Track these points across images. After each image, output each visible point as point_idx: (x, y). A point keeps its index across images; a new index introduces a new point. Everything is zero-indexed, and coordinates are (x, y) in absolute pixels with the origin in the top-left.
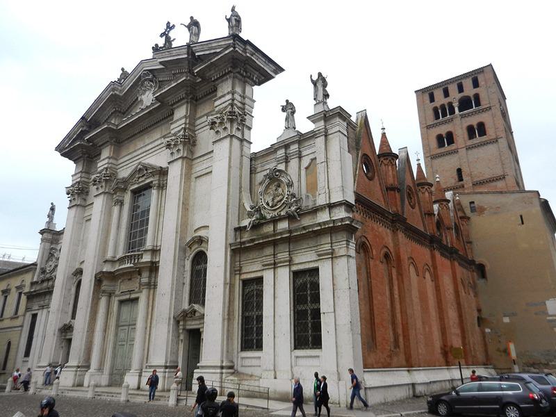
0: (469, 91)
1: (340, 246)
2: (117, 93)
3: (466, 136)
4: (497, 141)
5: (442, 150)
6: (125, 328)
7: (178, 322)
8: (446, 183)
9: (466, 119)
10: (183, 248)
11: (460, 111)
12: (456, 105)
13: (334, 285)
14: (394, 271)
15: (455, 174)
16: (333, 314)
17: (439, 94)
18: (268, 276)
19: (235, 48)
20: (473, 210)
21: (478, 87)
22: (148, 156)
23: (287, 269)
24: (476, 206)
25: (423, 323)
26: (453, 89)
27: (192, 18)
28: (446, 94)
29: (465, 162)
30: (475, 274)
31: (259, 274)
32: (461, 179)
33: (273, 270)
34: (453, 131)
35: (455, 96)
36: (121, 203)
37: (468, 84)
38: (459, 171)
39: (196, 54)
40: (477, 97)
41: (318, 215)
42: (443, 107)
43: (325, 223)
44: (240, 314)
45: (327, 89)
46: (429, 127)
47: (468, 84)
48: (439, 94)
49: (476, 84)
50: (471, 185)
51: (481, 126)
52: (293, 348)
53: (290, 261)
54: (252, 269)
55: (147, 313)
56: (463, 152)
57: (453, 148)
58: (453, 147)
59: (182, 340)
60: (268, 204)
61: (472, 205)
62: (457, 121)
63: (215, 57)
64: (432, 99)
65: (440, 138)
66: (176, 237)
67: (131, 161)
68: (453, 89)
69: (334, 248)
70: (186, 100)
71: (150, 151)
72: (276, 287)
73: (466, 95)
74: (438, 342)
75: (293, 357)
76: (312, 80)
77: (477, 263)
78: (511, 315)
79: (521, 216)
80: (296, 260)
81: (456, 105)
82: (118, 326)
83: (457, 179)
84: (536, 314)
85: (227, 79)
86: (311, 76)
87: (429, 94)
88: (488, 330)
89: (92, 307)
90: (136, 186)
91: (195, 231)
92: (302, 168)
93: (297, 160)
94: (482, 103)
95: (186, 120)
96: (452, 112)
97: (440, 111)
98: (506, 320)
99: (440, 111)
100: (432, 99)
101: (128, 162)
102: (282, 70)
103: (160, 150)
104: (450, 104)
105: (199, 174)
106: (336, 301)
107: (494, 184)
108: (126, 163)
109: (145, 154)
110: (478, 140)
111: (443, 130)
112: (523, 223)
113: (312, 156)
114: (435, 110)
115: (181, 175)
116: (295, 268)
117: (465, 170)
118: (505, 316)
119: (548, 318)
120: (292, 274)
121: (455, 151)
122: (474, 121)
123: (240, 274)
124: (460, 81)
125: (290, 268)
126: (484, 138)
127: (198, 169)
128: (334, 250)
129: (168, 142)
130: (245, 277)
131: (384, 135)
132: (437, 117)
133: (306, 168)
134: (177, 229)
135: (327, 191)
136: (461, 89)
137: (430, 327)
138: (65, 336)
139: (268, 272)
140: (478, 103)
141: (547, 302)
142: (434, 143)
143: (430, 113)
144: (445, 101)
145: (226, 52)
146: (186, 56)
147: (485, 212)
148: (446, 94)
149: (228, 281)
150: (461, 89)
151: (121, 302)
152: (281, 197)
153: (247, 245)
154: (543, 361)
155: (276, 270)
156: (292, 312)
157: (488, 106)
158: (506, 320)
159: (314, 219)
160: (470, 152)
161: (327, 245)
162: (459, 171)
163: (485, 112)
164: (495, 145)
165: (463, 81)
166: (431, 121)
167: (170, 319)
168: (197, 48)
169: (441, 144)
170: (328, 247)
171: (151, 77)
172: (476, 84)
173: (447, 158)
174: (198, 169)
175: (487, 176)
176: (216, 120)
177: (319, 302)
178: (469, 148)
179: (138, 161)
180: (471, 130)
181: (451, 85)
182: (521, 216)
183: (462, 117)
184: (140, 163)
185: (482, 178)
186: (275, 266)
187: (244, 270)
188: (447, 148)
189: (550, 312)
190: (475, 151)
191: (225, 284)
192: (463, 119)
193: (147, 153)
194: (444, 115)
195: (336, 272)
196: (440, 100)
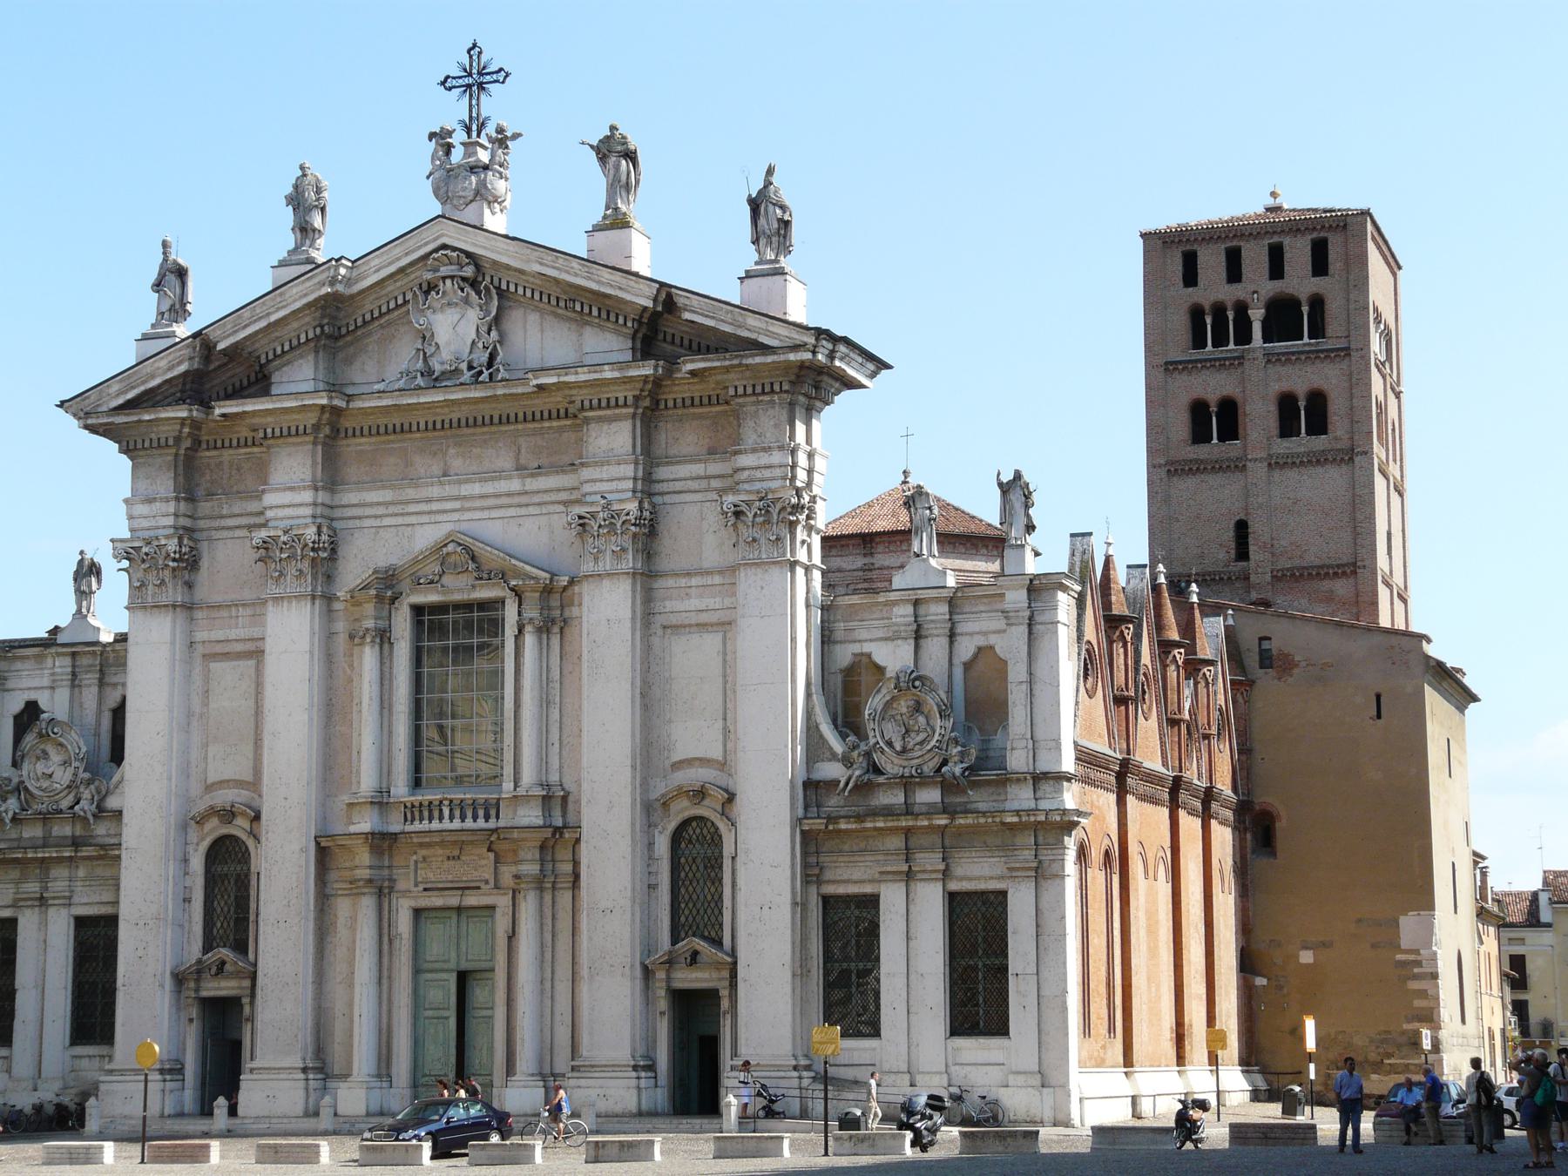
0: (1299, 282)
1: (1051, 857)
2: (340, 288)
3: (1273, 423)
4: (1351, 459)
5: (1202, 451)
6: (445, 976)
7: (647, 972)
8: (1202, 556)
9: (1279, 368)
10: (650, 809)
11: (1266, 339)
12: (1257, 315)
13: (1037, 926)
14: (1116, 879)
15: (1229, 535)
16: (1035, 977)
17: (1211, 263)
18: (892, 898)
19: (814, 353)
20: (1266, 660)
21: (1326, 274)
22: (468, 515)
23: (939, 886)
24: (1274, 652)
25: (1149, 979)
26: (1255, 258)
27: (613, 128)
28: (1234, 272)
29: (1260, 506)
30: (1249, 836)
31: (868, 889)
32: (1242, 553)
33: (904, 884)
34: (1239, 401)
35: (1257, 288)
36: (384, 637)
37: (1298, 254)
38: (1242, 528)
39: (687, 316)
40: (1317, 303)
41: (1009, 789)
42: (1219, 311)
43: (1029, 812)
44: (821, 966)
45: (1031, 511)
46: (1171, 367)
47: (1298, 254)
48: (1211, 263)
49: (1320, 265)
50: (1268, 577)
51: (1318, 401)
52: (948, 1034)
53: (947, 870)
54: (849, 877)
55: (542, 945)
56: (1258, 471)
57: (1233, 454)
58: (1233, 448)
59: (662, 1013)
60: (890, 744)
61: (1266, 645)
62: (1255, 370)
63: (753, 356)
64: (1190, 278)
65: (1199, 410)
66: (634, 778)
67: (392, 509)
68: (1255, 258)
69: (1041, 858)
70: (624, 411)
71: (478, 503)
72: (910, 917)
73: (1290, 291)
74: (1168, 1018)
75: (950, 1049)
76: (1000, 485)
77: (1257, 808)
78: (1319, 946)
79: (1378, 697)
80: (958, 871)
81: (1257, 315)
82: (417, 971)
83: (1233, 556)
84: (1374, 946)
85: (772, 402)
86: (999, 474)
87: (1183, 252)
88: (1260, 981)
89: (316, 919)
90: (432, 598)
91: (677, 766)
92: (956, 661)
93: (945, 641)
94: (1329, 331)
95: (636, 470)
96: (1244, 337)
97: (1209, 320)
98: (1306, 957)
99: (1209, 320)
100: (1190, 278)
101: (381, 511)
102: (888, 367)
103: (523, 511)
104: (1242, 309)
105: (674, 620)
106: (1041, 956)
107: (1326, 585)
108: (381, 511)
109: (457, 505)
110: (1304, 443)
111: (1213, 386)
112: (1379, 716)
113: (980, 641)
114: (1197, 314)
115: (633, 619)
116: (954, 886)
117: (1257, 528)
118: (1306, 948)
119: (1399, 957)
120: (947, 896)
121: (1238, 466)
122: (1300, 380)
123: (819, 883)
124: (1276, 239)
125: (944, 886)
126: (1320, 442)
127: (670, 605)
128: (1040, 862)
129: (580, 517)
130: (830, 889)
131: (1108, 561)
132: (1199, 342)
133: (965, 664)
134: (634, 758)
135: (1030, 746)
136: (1277, 269)
137: (1158, 989)
138: (197, 990)
139: (890, 885)
140: (1317, 331)
141: (1403, 920)
142: (1181, 425)
143: (1180, 323)
144: (1229, 294)
145: (792, 357)
146: (650, 304)
147: (1296, 671)
148: (1234, 272)
149: (799, 899)
150: (1277, 269)
151: (417, 912)
152: (922, 736)
153: (843, 826)
154: (1373, 1056)
155: (912, 884)
156: (947, 968)
157: (1341, 344)
158: (1306, 957)
159: (999, 794)
160: (1277, 475)
161: (1026, 852)
162: (1242, 528)
163: (1332, 360)
164: (1344, 468)
165: (1287, 241)
166: (1180, 348)
167: (632, 966)
168: (695, 303)
169: (1200, 435)
170: (1028, 854)
171: (469, 271)
172: (1320, 265)
173: (1214, 480)
174: (670, 605)
175: (1311, 559)
176: (744, 507)
177: (1004, 953)
178: (1277, 464)
179: (444, 529)
180: (1287, 403)
181: (1252, 243)
182: (1378, 697)
183: (1271, 359)
184: (449, 534)
185: (1297, 562)
186: (909, 877)
187: (828, 875)
188: (1215, 448)
189: (1405, 943)
190: (1292, 474)
191: (794, 904)
192: (1270, 366)
193: (467, 505)
194: (1220, 341)
195: (1044, 904)
196: (1213, 288)
